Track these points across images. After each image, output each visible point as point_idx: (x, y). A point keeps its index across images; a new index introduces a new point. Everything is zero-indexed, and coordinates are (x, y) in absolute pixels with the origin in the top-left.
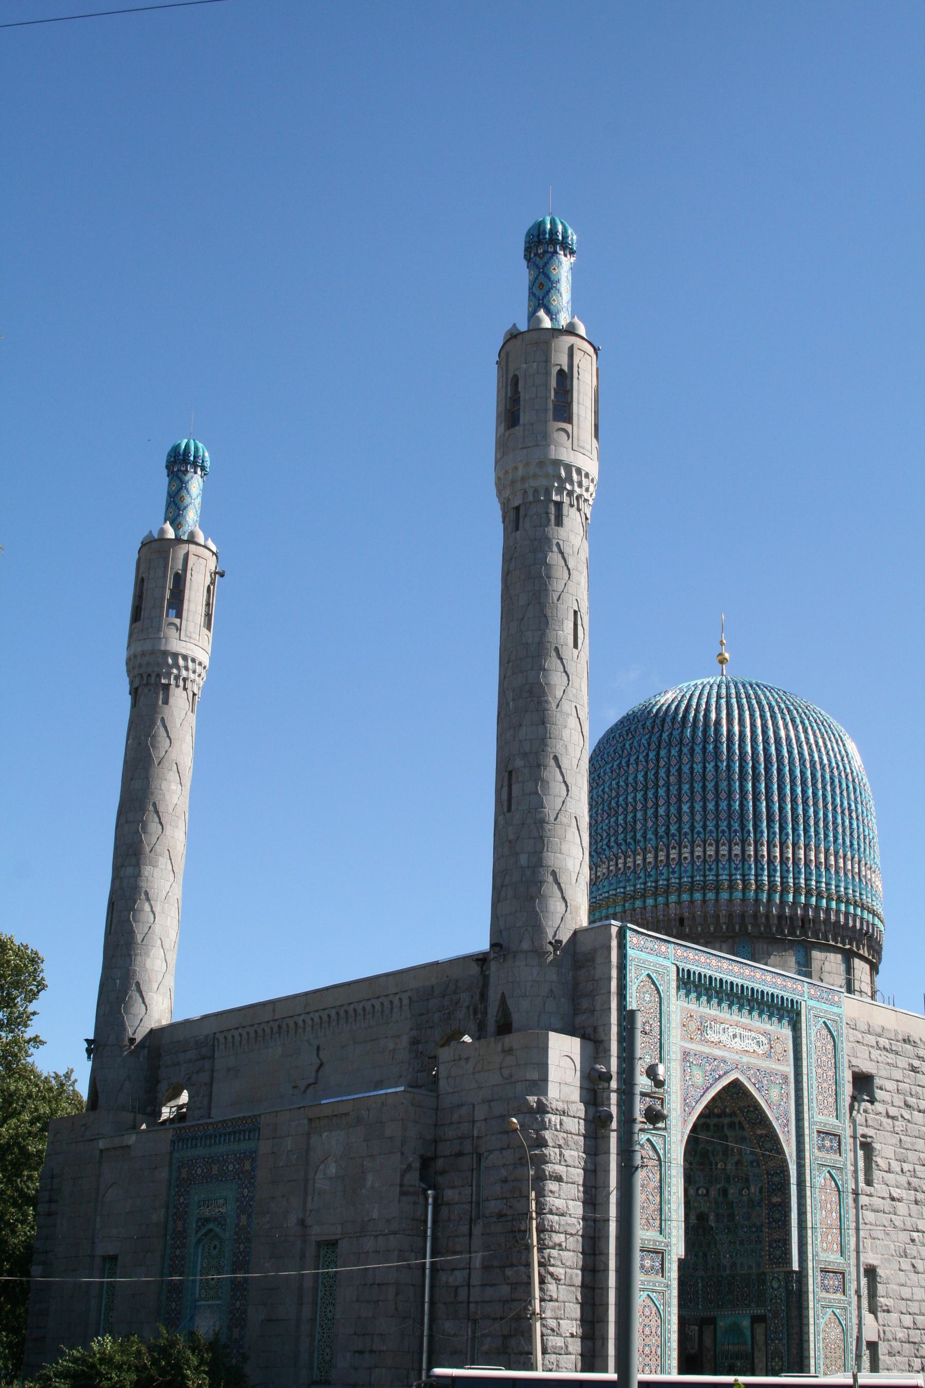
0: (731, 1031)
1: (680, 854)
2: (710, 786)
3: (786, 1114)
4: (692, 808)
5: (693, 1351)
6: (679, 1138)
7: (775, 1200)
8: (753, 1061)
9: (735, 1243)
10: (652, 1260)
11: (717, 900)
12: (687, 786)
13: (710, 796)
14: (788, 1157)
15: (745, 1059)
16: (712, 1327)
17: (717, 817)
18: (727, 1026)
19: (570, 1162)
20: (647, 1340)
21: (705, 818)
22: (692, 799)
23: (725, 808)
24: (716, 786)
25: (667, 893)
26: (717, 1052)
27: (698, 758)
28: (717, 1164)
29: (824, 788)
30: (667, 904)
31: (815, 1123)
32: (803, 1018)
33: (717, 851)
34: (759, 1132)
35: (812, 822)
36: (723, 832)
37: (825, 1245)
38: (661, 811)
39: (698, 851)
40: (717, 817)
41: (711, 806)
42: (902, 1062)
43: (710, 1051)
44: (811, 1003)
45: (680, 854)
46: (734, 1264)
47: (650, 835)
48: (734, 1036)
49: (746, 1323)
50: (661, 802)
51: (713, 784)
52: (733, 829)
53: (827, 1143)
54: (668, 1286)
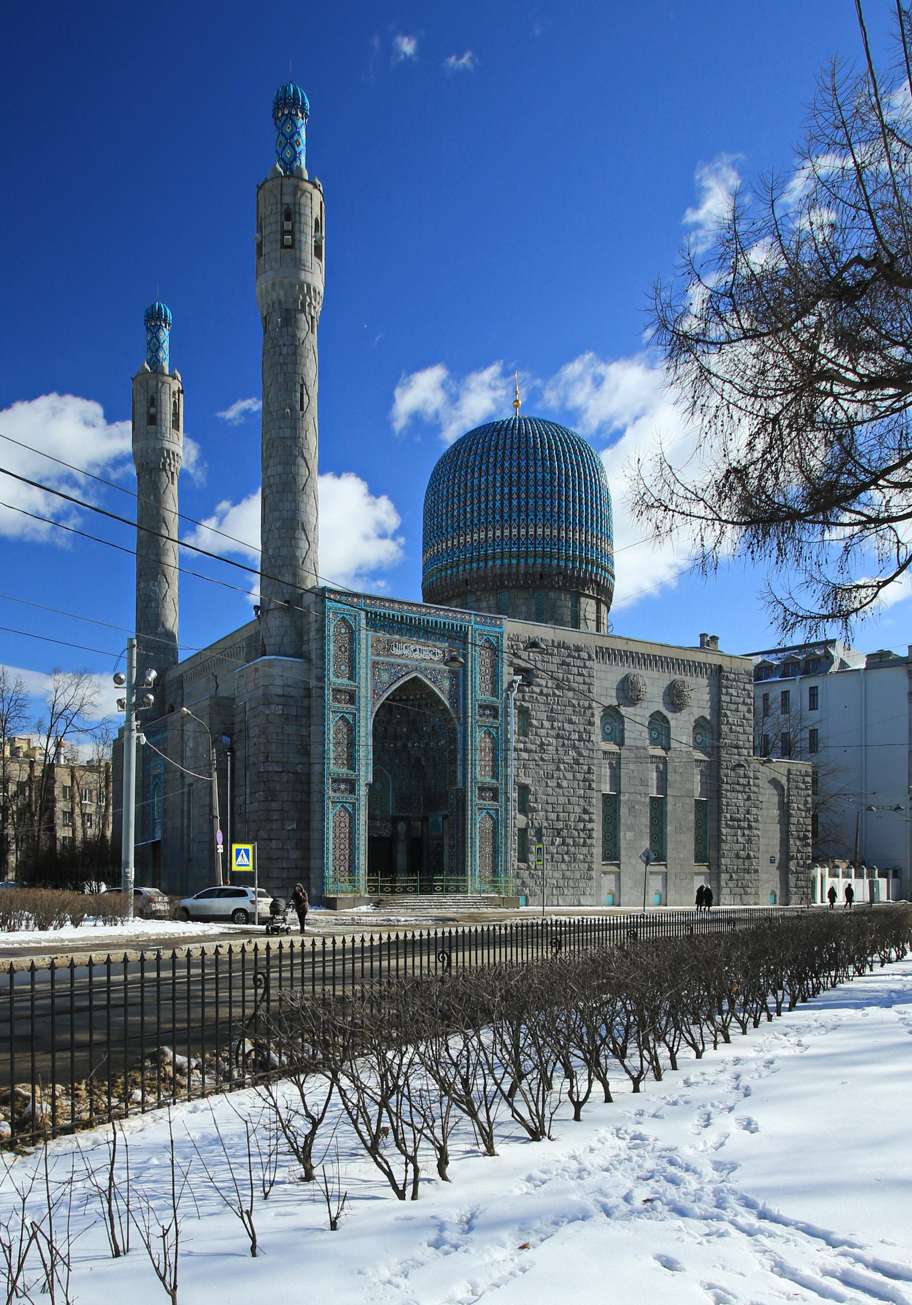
0: (412, 648)
1: (465, 539)
2: (483, 493)
4: (472, 508)
7: (452, 747)
11: (486, 567)
13: (483, 499)
15: (423, 664)
17: (487, 513)
21: (479, 515)
22: (472, 503)
25: (458, 565)
26: (400, 661)
27: (476, 475)
30: (458, 572)
33: (486, 535)
35: (548, 509)
36: (490, 522)
38: (455, 514)
39: (476, 537)
42: (556, 660)
44: (476, 626)
45: (465, 539)
47: (449, 530)
48: (415, 650)
49: (440, 819)
50: (456, 506)
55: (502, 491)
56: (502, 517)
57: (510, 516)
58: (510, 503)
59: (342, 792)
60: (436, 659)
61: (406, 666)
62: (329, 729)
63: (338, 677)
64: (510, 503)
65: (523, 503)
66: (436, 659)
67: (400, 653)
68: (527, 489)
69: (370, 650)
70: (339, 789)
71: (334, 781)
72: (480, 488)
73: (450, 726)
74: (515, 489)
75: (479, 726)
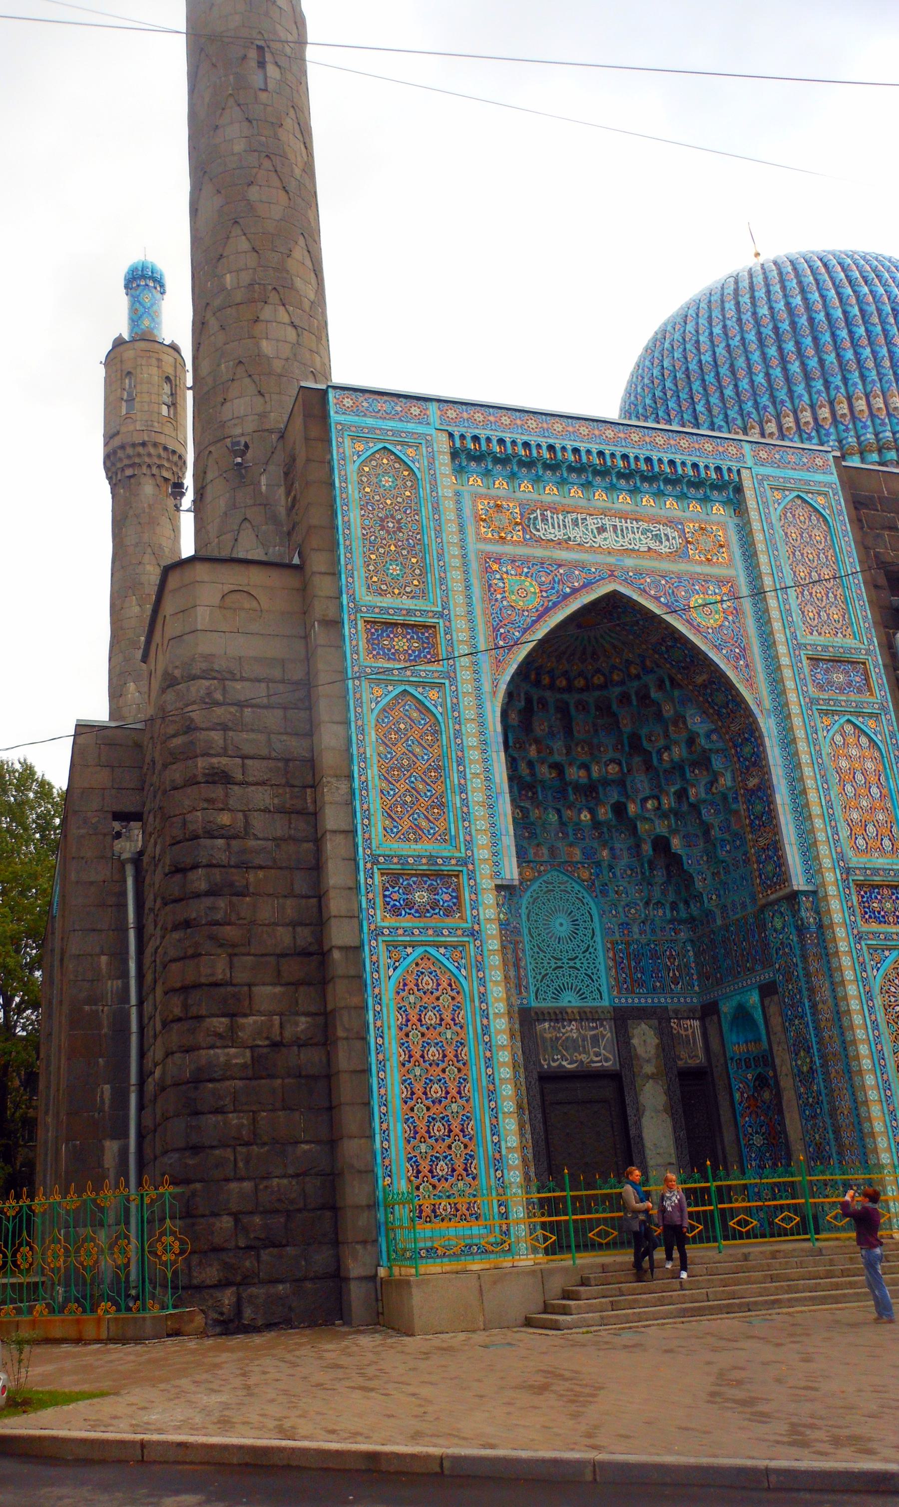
2: (724, 370)
6: (487, 687)
9: (718, 872)
10: (433, 890)
12: (698, 383)
13: (727, 380)
14: (754, 707)
15: (629, 562)
16: (715, 1018)
18: (584, 516)
19: (247, 749)
20: (431, 1035)
23: (747, 387)
24: (732, 369)
26: (563, 555)
28: (660, 753)
29: (883, 322)
32: (749, 493)
35: (870, 364)
40: (740, 402)
41: (729, 392)
44: (762, 470)
51: (727, 366)
52: (761, 406)
54: (473, 934)
55: (764, 355)
56: (773, 398)
57: (791, 392)
58: (785, 370)
59: (421, 913)
60: (664, 549)
61: (582, 566)
62: (362, 730)
63: (382, 593)
64: (785, 370)
65: (813, 363)
66: (664, 549)
67: (559, 535)
68: (815, 340)
69: (470, 530)
70: (409, 905)
71: (393, 878)
72: (716, 365)
73: (734, 728)
74: (790, 346)
75: (820, 711)
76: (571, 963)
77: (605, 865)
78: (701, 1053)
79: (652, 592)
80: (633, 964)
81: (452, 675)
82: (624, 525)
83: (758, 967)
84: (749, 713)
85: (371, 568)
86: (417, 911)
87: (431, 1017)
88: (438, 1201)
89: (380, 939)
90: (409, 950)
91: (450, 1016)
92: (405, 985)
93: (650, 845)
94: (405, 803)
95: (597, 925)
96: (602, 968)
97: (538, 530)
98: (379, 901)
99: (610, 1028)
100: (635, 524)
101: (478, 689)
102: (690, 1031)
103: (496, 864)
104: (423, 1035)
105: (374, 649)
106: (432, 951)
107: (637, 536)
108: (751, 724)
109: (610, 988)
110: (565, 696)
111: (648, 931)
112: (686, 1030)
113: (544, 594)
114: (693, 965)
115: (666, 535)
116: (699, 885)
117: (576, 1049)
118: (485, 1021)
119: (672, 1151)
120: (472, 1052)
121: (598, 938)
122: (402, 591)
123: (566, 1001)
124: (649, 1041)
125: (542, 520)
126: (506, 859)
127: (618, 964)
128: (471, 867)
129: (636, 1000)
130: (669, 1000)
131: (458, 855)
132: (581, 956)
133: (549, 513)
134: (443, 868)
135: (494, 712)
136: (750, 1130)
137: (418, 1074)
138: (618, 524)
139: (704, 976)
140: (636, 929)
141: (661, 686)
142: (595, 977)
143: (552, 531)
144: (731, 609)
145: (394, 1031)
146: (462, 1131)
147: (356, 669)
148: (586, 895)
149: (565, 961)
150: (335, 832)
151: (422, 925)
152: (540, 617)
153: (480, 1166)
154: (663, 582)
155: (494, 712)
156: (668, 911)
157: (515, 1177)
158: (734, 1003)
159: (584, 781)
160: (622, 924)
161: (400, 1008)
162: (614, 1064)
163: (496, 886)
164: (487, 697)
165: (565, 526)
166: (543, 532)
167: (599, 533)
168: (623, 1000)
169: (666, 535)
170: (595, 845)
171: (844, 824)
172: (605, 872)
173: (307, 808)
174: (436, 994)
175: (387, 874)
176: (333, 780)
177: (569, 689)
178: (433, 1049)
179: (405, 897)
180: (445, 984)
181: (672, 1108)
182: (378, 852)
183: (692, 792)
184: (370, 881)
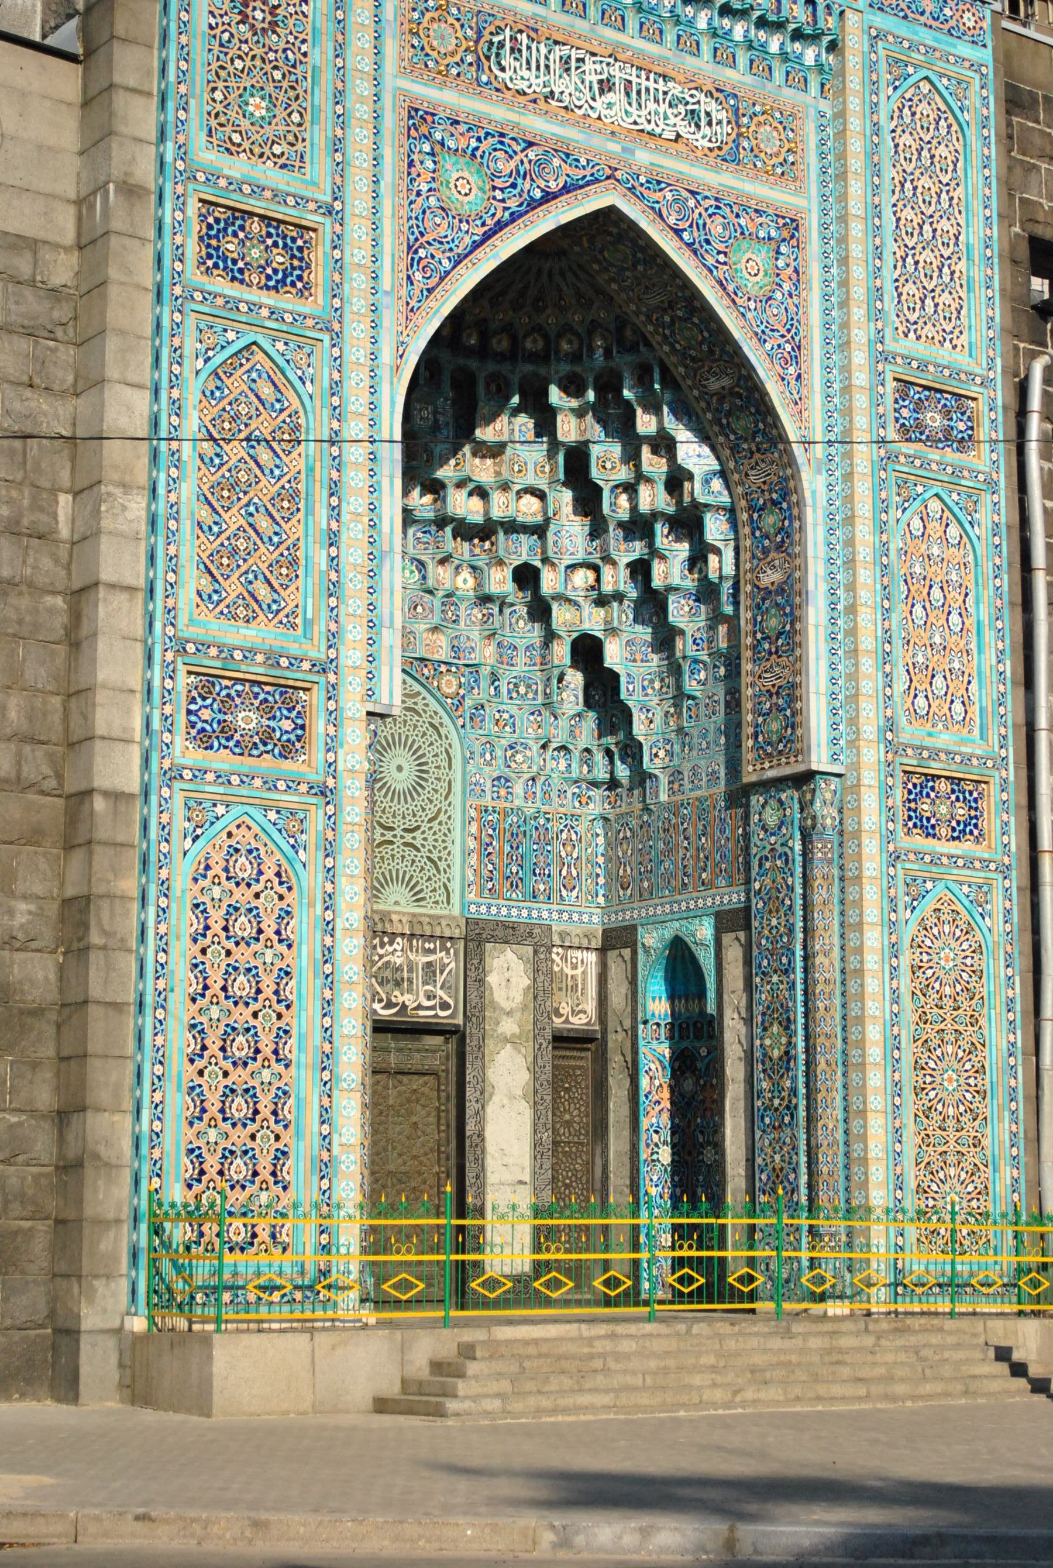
3: (792, 326)
5: (578, 1022)
6: (387, 356)
7: (770, 578)
8: (672, 165)
10: (266, 709)
15: (643, 157)
16: (627, 953)
20: (243, 955)
26: (536, 124)
31: (887, 357)
34: (714, 385)
37: (921, 701)
43: (513, 117)
46: (676, 775)
48: (606, 86)
49: (705, 930)
53: (934, 420)
63: (231, 149)
69: (391, 48)
70: (226, 731)
71: (207, 684)
76: (408, 837)
77: (485, 671)
78: (590, 1006)
79: (672, 221)
80: (507, 849)
81: (336, 327)
82: (645, 83)
83: (721, 882)
84: (791, 462)
85: (218, 95)
86: (238, 744)
87: (242, 926)
88: (280, 1221)
89: (177, 785)
90: (220, 810)
91: (274, 927)
92: (208, 867)
93: (567, 649)
94: (235, 551)
95: (457, 774)
96: (456, 850)
97: (503, 69)
98: (181, 719)
99: (456, 954)
100: (661, 86)
101: (374, 356)
102: (580, 970)
103: (370, 676)
104: (229, 953)
105: (210, 256)
106: (257, 813)
107: (661, 110)
108: (786, 479)
109: (465, 885)
110: (473, 364)
111: (539, 795)
112: (574, 967)
113: (498, 194)
114: (601, 860)
115: (708, 114)
116: (639, 729)
117: (398, 984)
118: (328, 941)
119: (526, 1161)
120: (305, 988)
121: (456, 798)
122: (267, 150)
123: (392, 899)
124: (513, 980)
125: (512, 50)
126: (385, 670)
127: (484, 849)
128: (332, 678)
129: (504, 911)
130: (555, 916)
131: (313, 654)
132: (425, 826)
133: (525, 41)
134: (288, 674)
135: (393, 403)
136: (655, 1138)
137: (215, 1016)
138: (634, 80)
139: (617, 882)
140: (519, 789)
141: (643, 379)
142: (442, 865)
143: (526, 74)
144: (790, 270)
145: (186, 941)
146: (275, 1113)
147: (178, 290)
148: (446, 720)
149: (399, 832)
150: (112, 586)
151: (245, 770)
152: (487, 237)
153: (296, 1169)
154: (691, 203)
155: (393, 403)
156: (575, 765)
157: (349, 1188)
158: (668, 934)
159: (478, 518)
160: (499, 778)
161: (197, 906)
162: (452, 1016)
163: (369, 714)
164: (384, 373)
165: (547, 67)
166: (509, 73)
167: (602, 92)
168: (483, 909)
169: (708, 114)
170: (475, 635)
171: (902, 671)
172: (484, 683)
173: (56, 531)
174: (256, 888)
175: (198, 674)
176: (117, 491)
177: (483, 352)
178: (241, 978)
179: (221, 717)
180: (270, 874)
181: (536, 1092)
182: (186, 635)
183: (658, 569)
184: (169, 684)
